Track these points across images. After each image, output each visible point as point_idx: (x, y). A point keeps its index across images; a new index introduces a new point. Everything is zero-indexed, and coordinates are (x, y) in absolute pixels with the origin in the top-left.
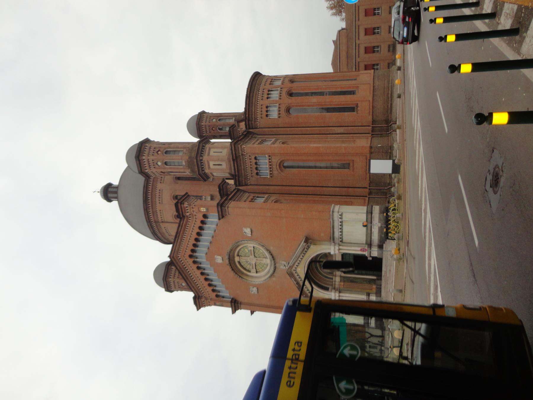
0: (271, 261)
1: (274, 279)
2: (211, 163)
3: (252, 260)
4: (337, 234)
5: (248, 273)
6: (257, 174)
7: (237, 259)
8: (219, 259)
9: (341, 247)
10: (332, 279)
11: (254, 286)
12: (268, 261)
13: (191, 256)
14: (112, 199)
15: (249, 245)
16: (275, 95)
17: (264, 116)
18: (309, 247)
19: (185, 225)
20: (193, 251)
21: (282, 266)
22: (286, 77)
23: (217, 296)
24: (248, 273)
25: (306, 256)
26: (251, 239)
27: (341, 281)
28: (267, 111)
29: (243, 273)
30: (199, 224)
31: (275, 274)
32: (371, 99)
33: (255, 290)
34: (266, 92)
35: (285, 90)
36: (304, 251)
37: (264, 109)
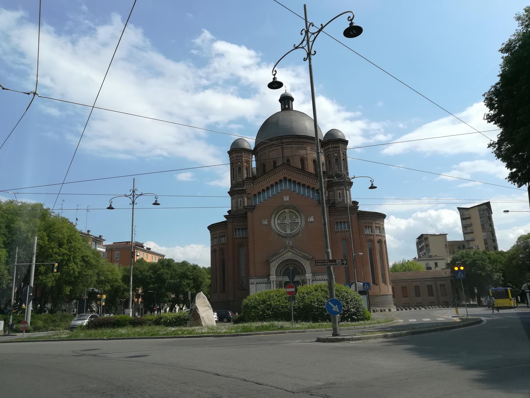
0: (290, 234)
1: (277, 237)
2: (340, 191)
3: (288, 221)
4: (318, 277)
5: (276, 218)
6: (337, 222)
7: (287, 210)
8: (286, 198)
9: (311, 281)
10: (280, 275)
11: (269, 222)
12: (289, 232)
13: (285, 178)
14: (282, 102)
15: (299, 219)
16: (377, 232)
17: (366, 225)
18: (308, 259)
19: (310, 177)
20: (290, 180)
21: (289, 242)
22: (385, 237)
23: (255, 195)
24: (276, 218)
25: (301, 258)
26: (306, 221)
27: (280, 281)
28: (369, 227)
29: (276, 215)
30: (312, 186)
31: (280, 237)
32: (381, 294)
33: (266, 223)
34: (379, 226)
35: (380, 238)
36: (304, 257)
37: (369, 225)
